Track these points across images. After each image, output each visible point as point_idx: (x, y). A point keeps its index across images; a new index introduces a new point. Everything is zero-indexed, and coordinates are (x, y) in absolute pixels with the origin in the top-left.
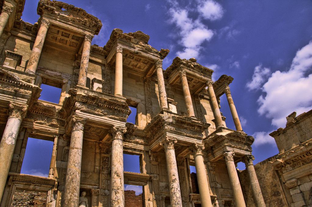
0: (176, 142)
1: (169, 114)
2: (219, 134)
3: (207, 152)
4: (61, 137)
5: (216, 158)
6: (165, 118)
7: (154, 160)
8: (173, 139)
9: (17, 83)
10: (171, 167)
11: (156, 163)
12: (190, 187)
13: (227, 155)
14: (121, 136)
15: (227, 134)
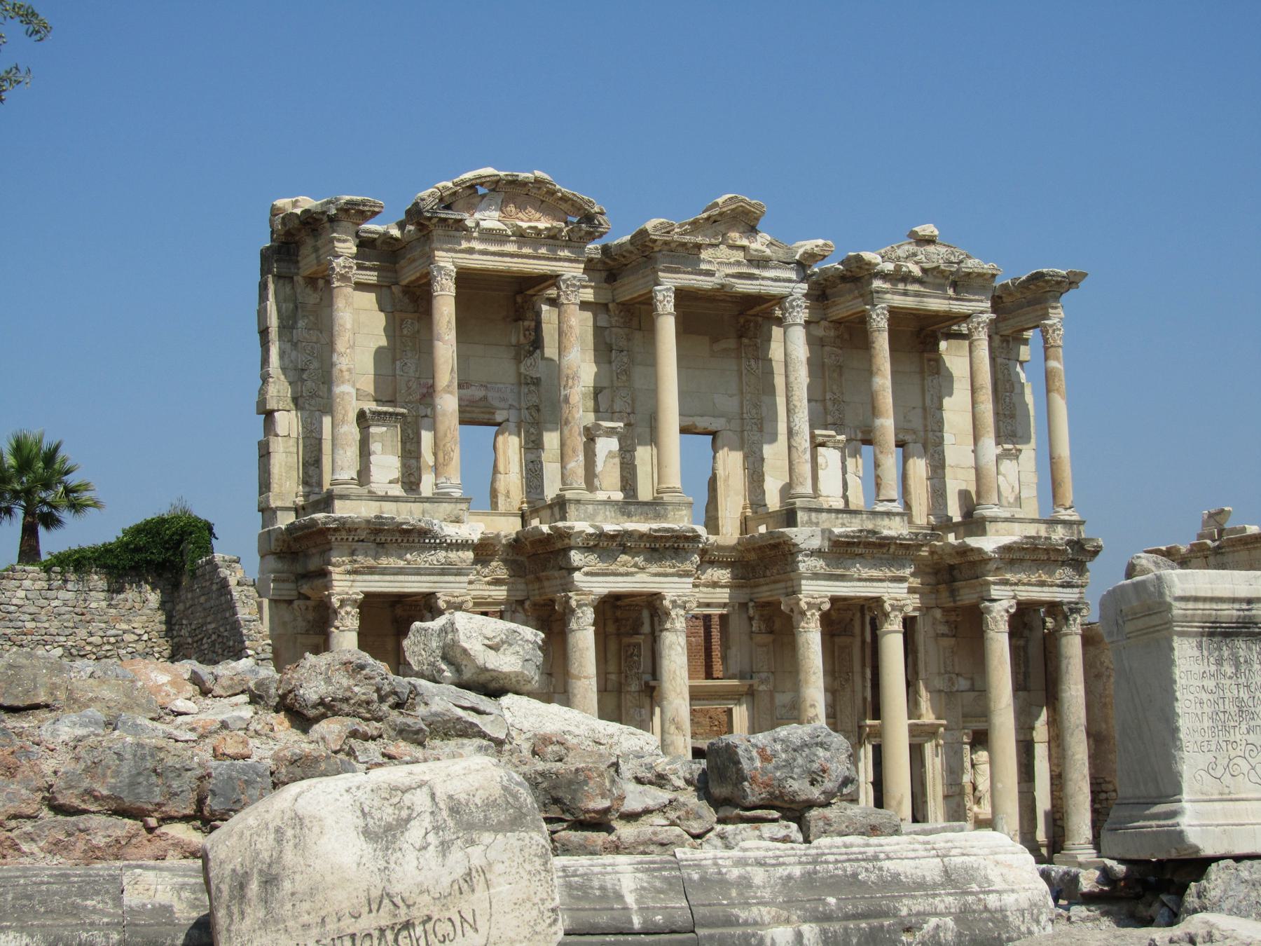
0: (826, 606)
1: (813, 515)
2: (973, 542)
3: (936, 572)
4: (520, 609)
5: (959, 603)
6: (796, 540)
7: (763, 627)
8: (819, 601)
9: (441, 543)
10: (807, 682)
11: (767, 638)
12: (865, 699)
13: (988, 610)
14: (683, 619)
15: (999, 548)
